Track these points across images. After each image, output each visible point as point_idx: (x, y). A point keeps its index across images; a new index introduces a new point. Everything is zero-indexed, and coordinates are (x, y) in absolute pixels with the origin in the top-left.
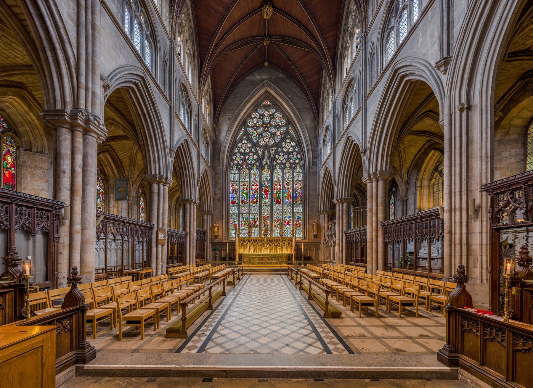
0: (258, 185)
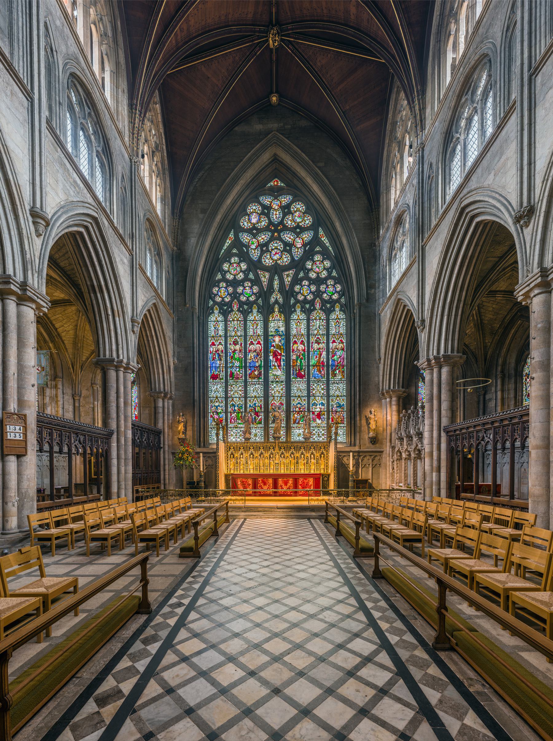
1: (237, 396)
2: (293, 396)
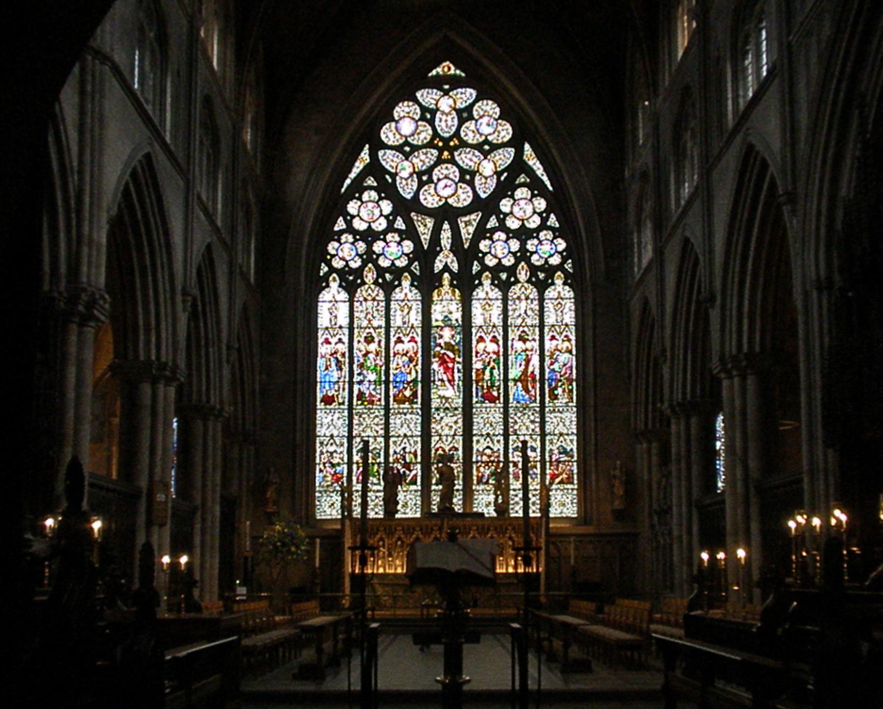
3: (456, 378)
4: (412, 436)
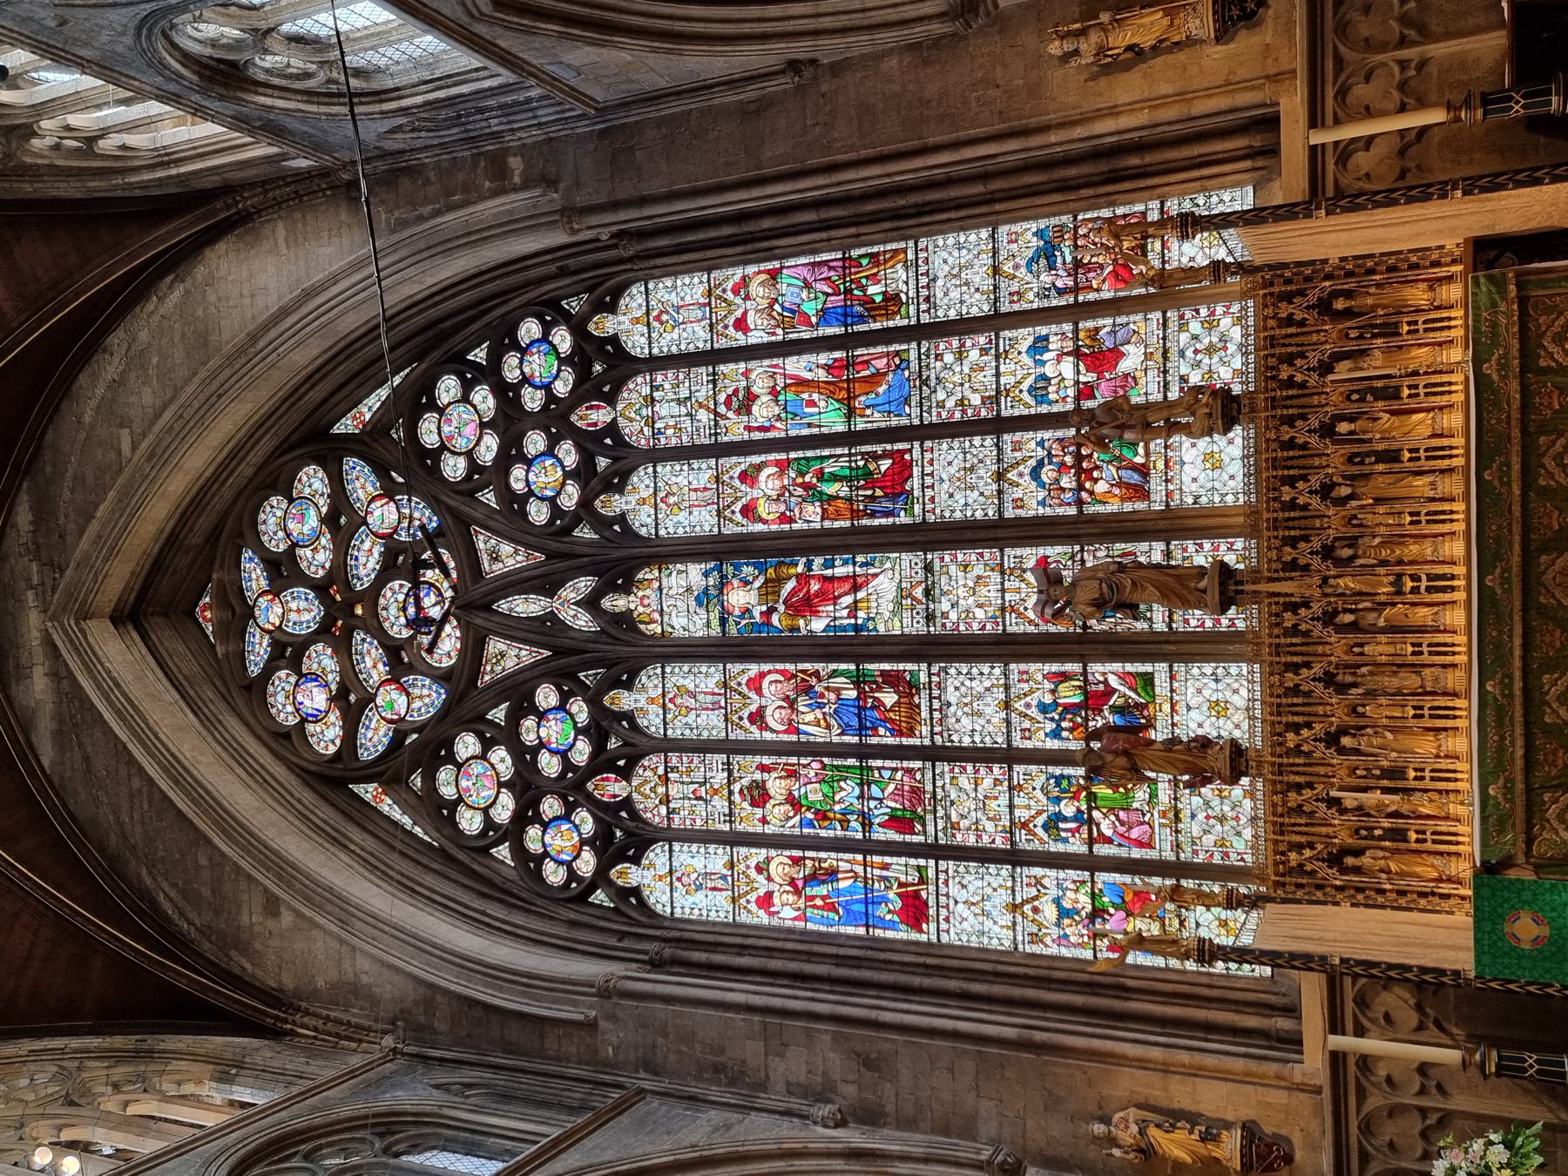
0: (754, 669)
1: (1004, 800)
2: (1000, 511)
3: (849, 569)
4: (1007, 687)
